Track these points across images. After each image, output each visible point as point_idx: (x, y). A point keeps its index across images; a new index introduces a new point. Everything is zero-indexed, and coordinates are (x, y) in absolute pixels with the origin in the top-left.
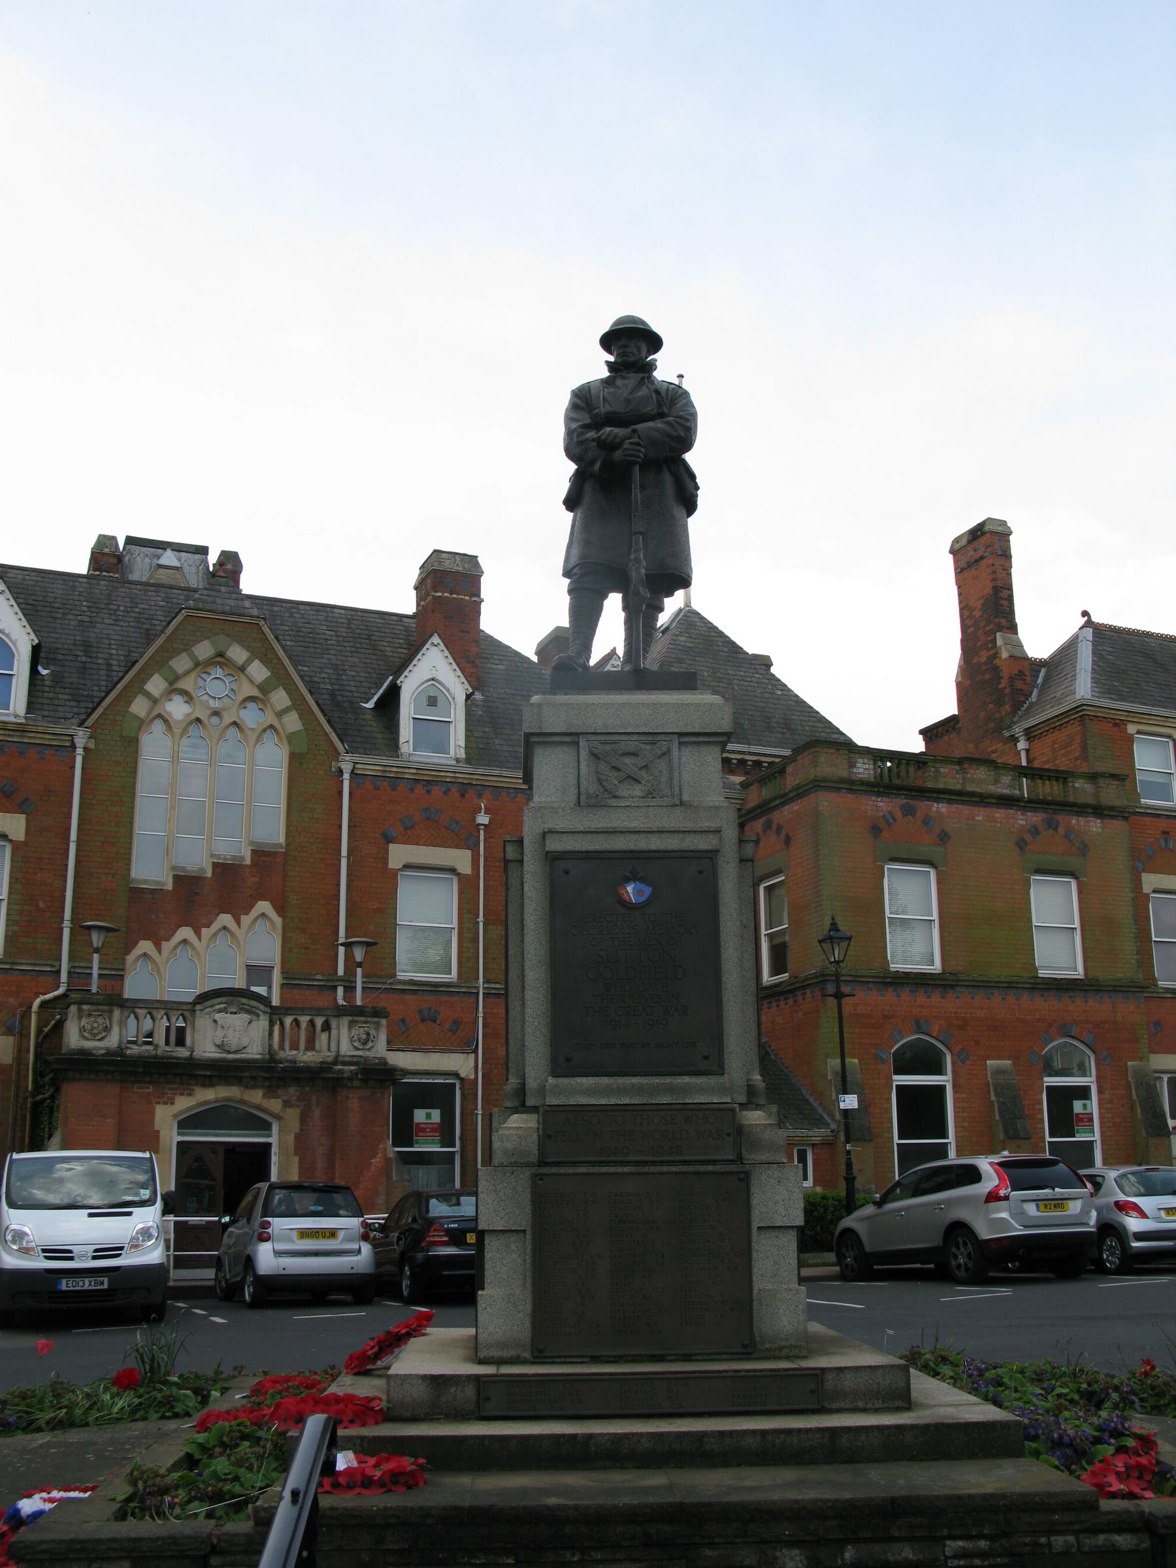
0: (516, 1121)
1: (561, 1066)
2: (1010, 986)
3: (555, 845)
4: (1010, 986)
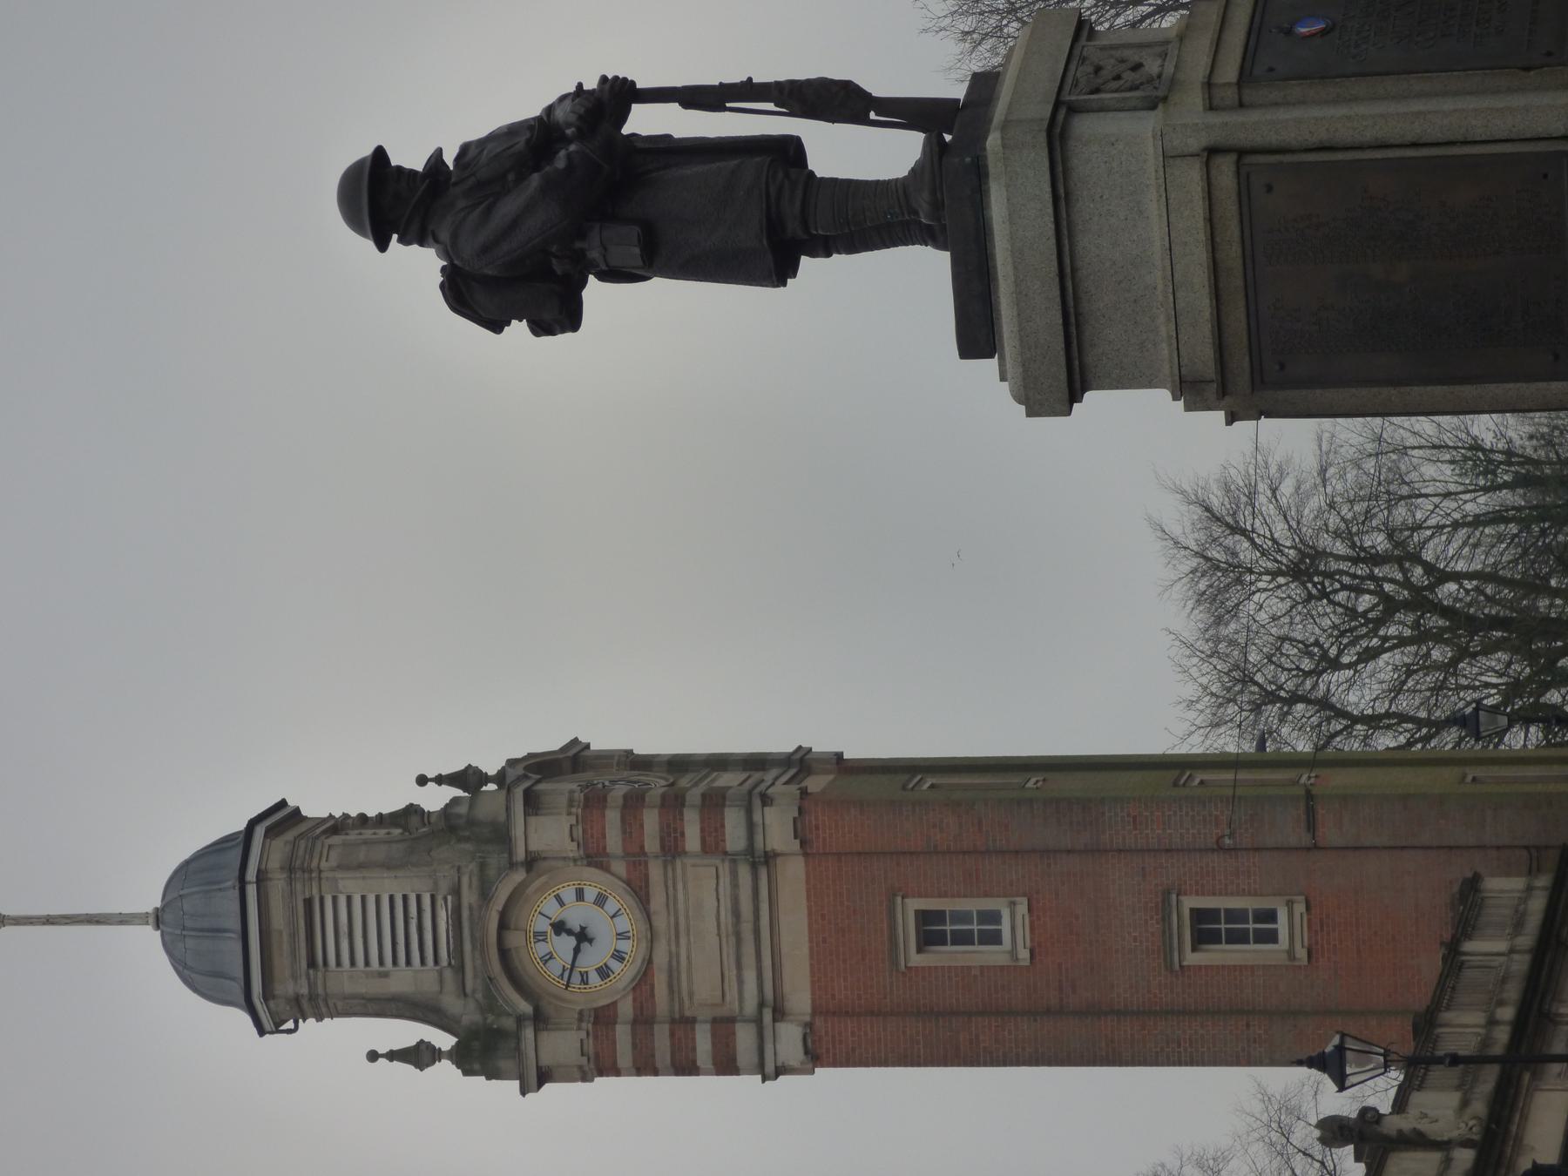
3: (1229, 71)
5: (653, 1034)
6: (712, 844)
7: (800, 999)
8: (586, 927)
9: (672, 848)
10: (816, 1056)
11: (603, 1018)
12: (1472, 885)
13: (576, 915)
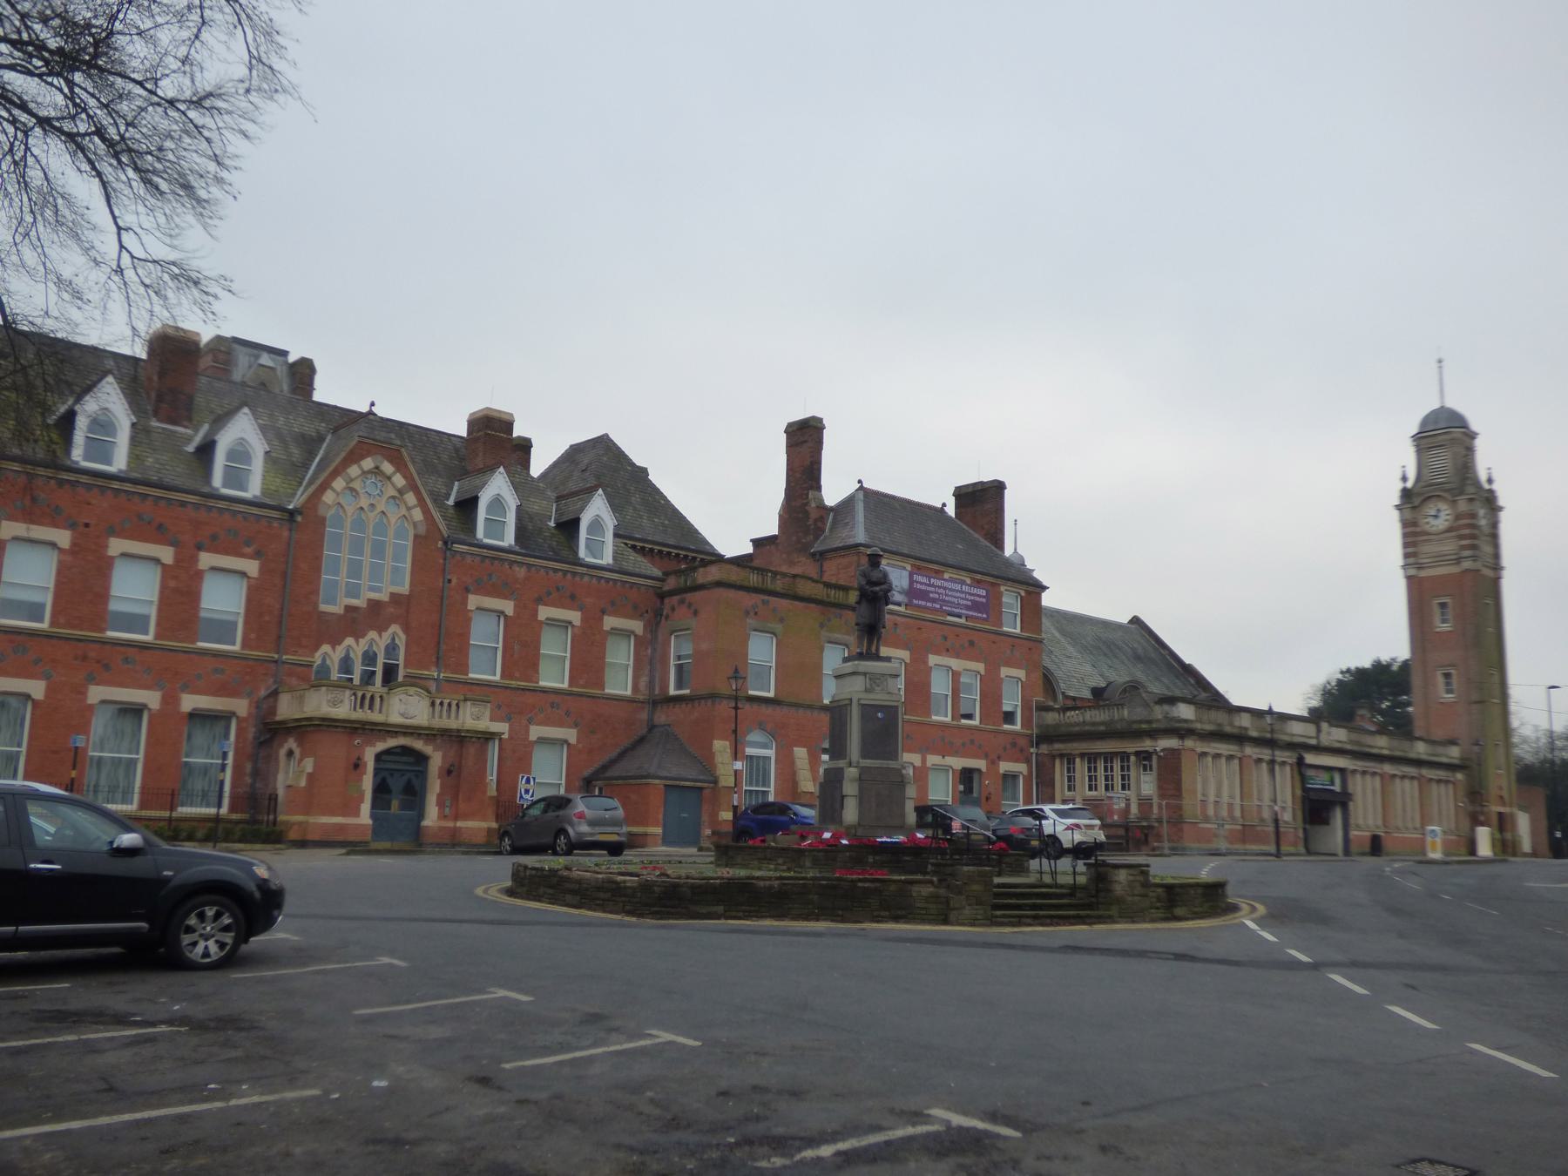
0: (852, 769)
1: (865, 755)
2: (810, 707)
4: (810, 707)
5: (1413, 536)
6: (1463, 548)
7: (1423, 574)
8: (1439, 517)
9: (1461, 537)
10: (1409, 578)
11: (1414, 524)
12: (1453, 742)
13: (1442, 514)
